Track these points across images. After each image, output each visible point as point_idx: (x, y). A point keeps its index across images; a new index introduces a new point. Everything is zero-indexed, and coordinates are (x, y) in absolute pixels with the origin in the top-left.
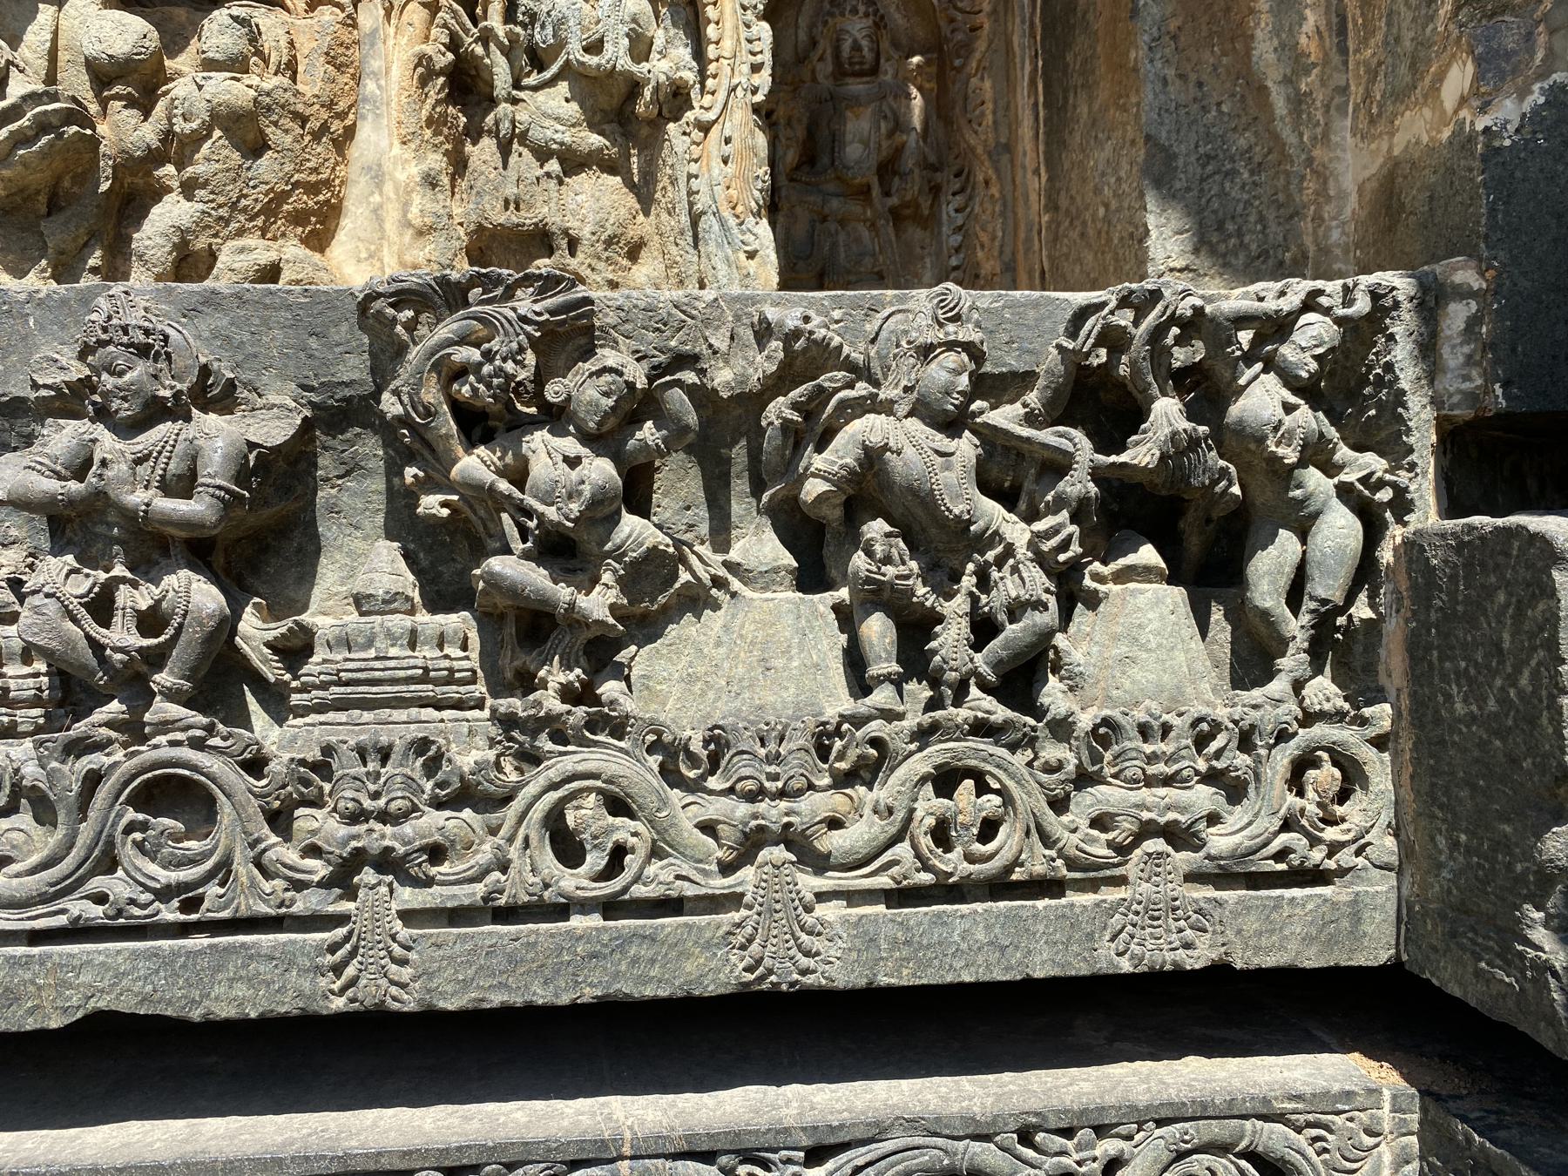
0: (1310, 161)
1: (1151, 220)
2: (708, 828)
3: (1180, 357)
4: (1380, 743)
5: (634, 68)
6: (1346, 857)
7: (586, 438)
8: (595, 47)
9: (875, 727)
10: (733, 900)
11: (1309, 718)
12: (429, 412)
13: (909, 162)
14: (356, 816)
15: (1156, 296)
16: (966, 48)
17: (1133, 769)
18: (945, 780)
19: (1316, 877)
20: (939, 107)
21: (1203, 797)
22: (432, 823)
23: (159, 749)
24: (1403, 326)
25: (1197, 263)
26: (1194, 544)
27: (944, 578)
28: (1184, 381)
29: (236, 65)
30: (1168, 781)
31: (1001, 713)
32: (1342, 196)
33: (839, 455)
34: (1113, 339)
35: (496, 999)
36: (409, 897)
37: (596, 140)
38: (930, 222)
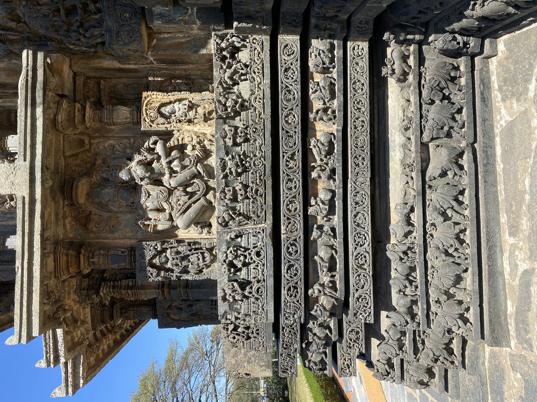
8: (185, 109)
13: (187, 82)
16: (173, 74)
18: (255, 73)
19: (263, 42)
20: (178, 79)
21: (256, 51)
22: (257, 112)
23: (251, 132)
24: (217, 33)
26: (235, 51)
27: (238, 72)
28: (221, 52)
29: (192, 137)
34: (219, 57)
36: (262, 114)
38: (194, 79)
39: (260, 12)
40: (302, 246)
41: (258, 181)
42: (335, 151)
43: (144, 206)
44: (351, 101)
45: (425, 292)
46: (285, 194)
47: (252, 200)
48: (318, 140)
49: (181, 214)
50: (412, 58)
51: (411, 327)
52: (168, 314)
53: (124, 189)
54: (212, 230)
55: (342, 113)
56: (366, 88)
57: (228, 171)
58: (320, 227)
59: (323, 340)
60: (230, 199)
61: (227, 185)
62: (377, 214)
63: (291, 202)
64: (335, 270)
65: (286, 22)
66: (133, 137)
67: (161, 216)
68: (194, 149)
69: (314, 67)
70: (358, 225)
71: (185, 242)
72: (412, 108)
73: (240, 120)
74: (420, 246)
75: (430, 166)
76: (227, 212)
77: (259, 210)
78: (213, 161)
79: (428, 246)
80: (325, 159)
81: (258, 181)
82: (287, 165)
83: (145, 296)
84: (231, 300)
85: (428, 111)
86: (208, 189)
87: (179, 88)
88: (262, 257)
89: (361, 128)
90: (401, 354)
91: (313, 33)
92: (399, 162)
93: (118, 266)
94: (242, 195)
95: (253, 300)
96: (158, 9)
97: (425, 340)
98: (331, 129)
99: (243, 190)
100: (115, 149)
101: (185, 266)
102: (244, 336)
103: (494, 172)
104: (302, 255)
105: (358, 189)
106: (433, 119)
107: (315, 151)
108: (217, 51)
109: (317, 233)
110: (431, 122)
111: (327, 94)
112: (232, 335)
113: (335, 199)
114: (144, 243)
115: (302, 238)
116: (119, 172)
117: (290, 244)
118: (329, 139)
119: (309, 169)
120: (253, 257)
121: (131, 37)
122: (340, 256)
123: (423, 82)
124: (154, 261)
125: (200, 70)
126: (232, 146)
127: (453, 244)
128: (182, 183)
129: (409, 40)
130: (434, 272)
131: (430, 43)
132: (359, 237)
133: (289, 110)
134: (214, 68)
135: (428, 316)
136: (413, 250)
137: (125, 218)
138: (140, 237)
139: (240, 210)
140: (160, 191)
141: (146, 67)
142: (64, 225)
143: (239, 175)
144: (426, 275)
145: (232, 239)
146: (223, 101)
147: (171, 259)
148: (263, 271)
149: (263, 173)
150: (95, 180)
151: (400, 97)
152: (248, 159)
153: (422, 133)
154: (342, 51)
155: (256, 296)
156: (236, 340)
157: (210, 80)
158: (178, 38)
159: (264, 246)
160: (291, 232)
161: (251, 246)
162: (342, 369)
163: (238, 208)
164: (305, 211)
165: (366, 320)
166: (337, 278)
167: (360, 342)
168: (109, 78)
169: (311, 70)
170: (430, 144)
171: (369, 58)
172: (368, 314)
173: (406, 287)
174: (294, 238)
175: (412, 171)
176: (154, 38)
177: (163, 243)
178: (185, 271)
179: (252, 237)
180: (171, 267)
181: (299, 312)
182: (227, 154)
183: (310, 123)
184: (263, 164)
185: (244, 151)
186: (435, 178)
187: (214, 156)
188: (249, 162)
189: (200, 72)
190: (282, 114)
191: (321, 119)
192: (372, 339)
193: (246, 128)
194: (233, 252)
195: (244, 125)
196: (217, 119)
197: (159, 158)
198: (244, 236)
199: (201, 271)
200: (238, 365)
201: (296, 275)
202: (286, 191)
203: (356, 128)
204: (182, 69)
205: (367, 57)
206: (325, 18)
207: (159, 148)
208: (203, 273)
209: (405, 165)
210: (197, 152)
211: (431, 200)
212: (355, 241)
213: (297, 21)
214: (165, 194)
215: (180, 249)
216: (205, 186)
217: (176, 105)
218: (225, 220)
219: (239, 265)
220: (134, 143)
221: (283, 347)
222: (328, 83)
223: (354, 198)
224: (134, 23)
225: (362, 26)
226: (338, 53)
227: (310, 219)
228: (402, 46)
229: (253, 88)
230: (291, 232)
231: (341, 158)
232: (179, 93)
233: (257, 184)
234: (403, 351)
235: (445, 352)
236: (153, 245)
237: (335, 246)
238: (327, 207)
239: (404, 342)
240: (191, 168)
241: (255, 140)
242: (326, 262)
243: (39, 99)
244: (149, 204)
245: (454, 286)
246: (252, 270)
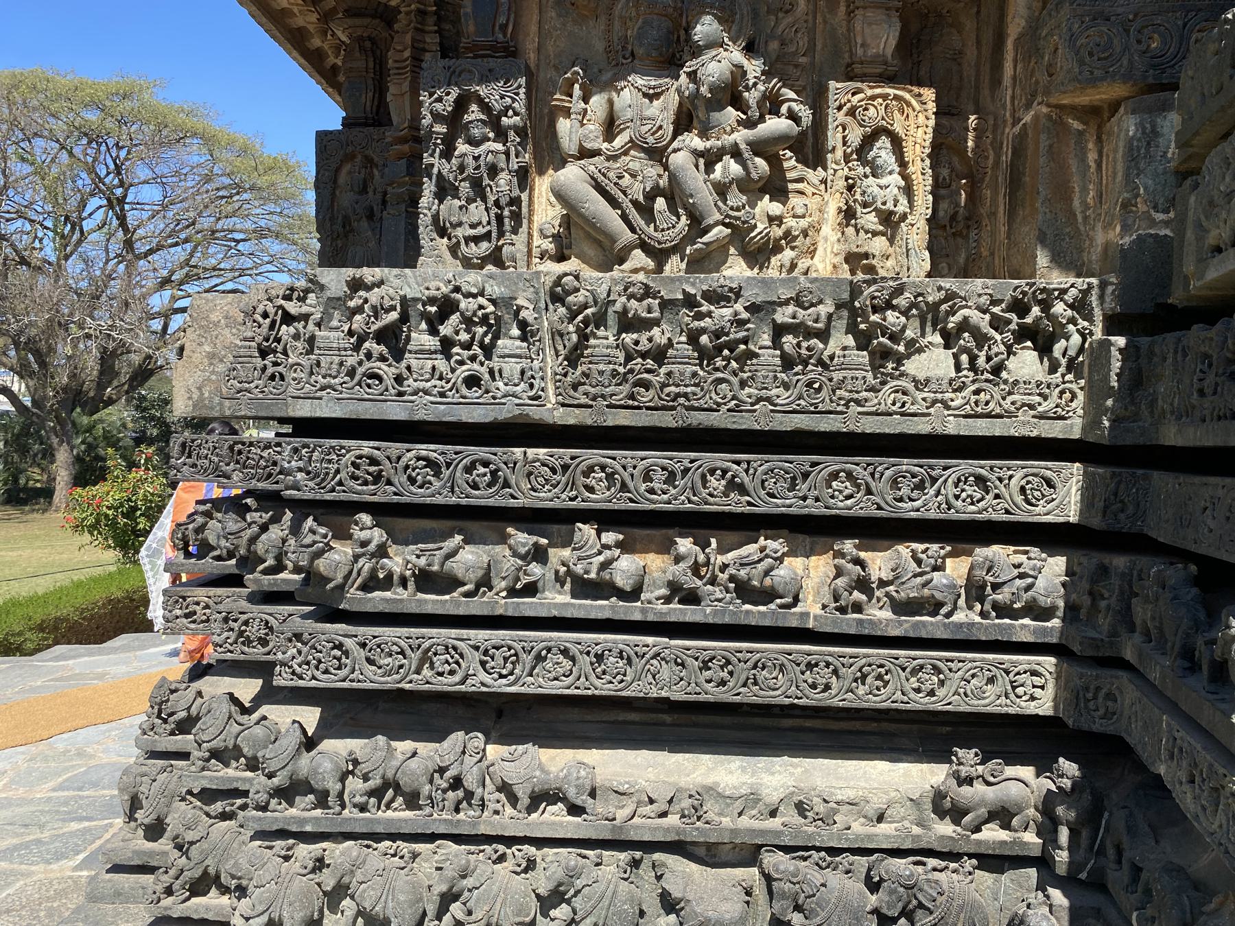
0: (1088, 236)
1: (1038, 253)
2: (924, 399)
3: (1040, 297)
4: (1081, 389)
5: (895, 209)
6: (1071, 414)
7: (900, 313)
8: (884, 203)
9: (963, 379)
10: (929, 415)
11: (1064, 383)
12: (867, 306)
13: (960, 218)
14: (851, 391)
15: (1035, 283)
16: (982, 180)
17: (1021, 391)
18: (977, 392)
20: (970, 197)
21: (1038, 399)
22: (864, 394)
24: (1095, 292)
25: (1051, 265)
26: (1040, 342)
27: (980, 348)
28: (1039, 302)
29: (803, 216)
30: (1029, 394)
31: (992, 377)
32: (1097, 246)
33: (958, 318)
34: (1024, 293)
35: (878, 431)
36: (860, 409)
37: (881, 228)
38: (966, 237)
39: (1152, 412)
40: (491, 502)
41: (672, 389)
42: (747, 607)
43: (623, 84)
44: (884, 657)
45: (348, 830)
46: (634, 462)
47: (621, 370)
48: (780, 560)
49: (592, 178)
50: (1004, 835)
51: (257, 783)
52: (350, 157)
53: (670, 32)
54: (549, 261)
55: (852, 631)
56: (921, 702)
57: (704, 309)
58: (539, 555)
59: (249, 550)
60: (625, 310)
61: (665, 305)
62: (574, 714)
63: (610, 477)
64: (420, 589)
65: (1119, 482)
66: (812, 64)
67: (594, 128)
68: (773, 220)
69: (986, 559)
70: (539, 659)
71: (522, 190)
72: (858, 827)
73: (845, 348)
74: (474, 825)
75: (694, 866)
76: (591, 300)
77: (592, 390)
78: (736, 270)
79: (472, 848)
80: (725, 576)
81: (672, 389)
82: (712, 472)
83: (395, 90)
84: (352, 304)
85: (847, 872)
86: (660, 255)
87: (943, 198)
88: (464, 391)
89: (810, 681)
90: (201, 754)
91: (1084, 560)
92: (709, 781)
93: (466, 14)
94: (637, 343)
95: (351, 361)
96: (1171, 123)
97: (234, 822)
98: (811, 598)
99: (649, 346)
100: (781, 15)
101: (457, 189)
102: (267, 340)
104: (464, 501)
105: (639, 664)
106: (823, 885)
107: (750, 549)
108: (1044, 290)
109: (524, 545)
110: (816, 877)
111: (911, 590)
112: (271, 310)
113: (614, 599)
114: (523, 81)
115: (512, 503)
116: (713, 15)
117: (497, 470)
118: (780, 590)
119: (702, 532)
120: (465, 367)
121: (1091, 54)
122: (458, 604)
123: (932, 862)
124: (474, 107)
125: (992, 254)
126: (773, 320)
127: (473, 917)
128: (679, 184)
129: (1056, 831)
130: (402, 857)
131: (1044, 890)
132: (506, 659)
133: (867, 484)
134: (993, 281)
135: (282, 834)
136: (464, 804)
137: (595, 38)
138: (542, 75)
139: (596, 337)
140: (660, 127)
141: (1005, 109)
143: (693, 338)
144: (393, 837)
145: (517, 313)
146: (901, 301)
147: (477, 151)
148: (426, 392)
151: (893, 794)
152: (734, 364)
153: (787, 849)
154: (1029, 638)
155: (360, 370)
156: (260, 319)
157: (965, 273)
158: (1085, 190)
159: (494, 398)
160: (529, 474)
161: (495, 363)
162: (184, 598)
163: (601, 333)
164: (587, 516)
165: (283, 664)
166: (399, 594)
167: (239, 647)
168: (978, 12)
169: (978, 550)
170: (755, 870)
171: (1007, 715)
172: (298, 670)
173: (366, 778)
174: (513, 482)
175: (683, 816)
176: (1084, 124)
177: (521, 132)
178: (445, 190)
179: (519, 367)
180: (456, 153)
181: (311, 484)
182: (753, 308)
183: (829, 540)
184: (719, 404)
185: (757, 356)
186: (659, 878)
187: (749, 273)
188: (725, 367)
189: (985, 253)
190: (859, 466)
191: (839, 573)
192: (260, 682)
193: (821, 362)
194: (480, 313)
195: (832, 358)
196: (852, 282)
197: (750, 124)
198: (525, 344)
199: (442, 232)
200: (206, 329)
201: (412, 480)
202: (642, 465)
203: (810, 666)
204: (997, 206)
205: (1011, 711)
206: (1127, 597)
207: (776, 125)
208: (435, 235)
209: (699, 799)
210: (760, 227)
211: (598, 864)
212: (497, 648)
213: (1122, 516)
214: (651, 140)
215: (503, 179)
216: (669, 245)
217: (895, 180)
218: (568, 293)
219: (445, 330)
220: (796, 66)
221: (236, 443)
222: (939, 596)
223: (615, 652)
224: (1131, 62)
225: (1100, 700)
226: (1025, 629)
227: (564, 528)
228: (1037, 809)
229: (934, 387)
230: (529, 474)
231: (727, 620)
232: (929, 188)
233: (664, 385)
234: (208, 760)
235: (197, 873)
236: (516, 105)
237: (485, 593)
238: (593, 575)
239: (234, 764)
240: (719, 209)
241: (786, 386)
242: (442, 565)
244: (627, 97)
245: (360, 913)
246: (429, 364)
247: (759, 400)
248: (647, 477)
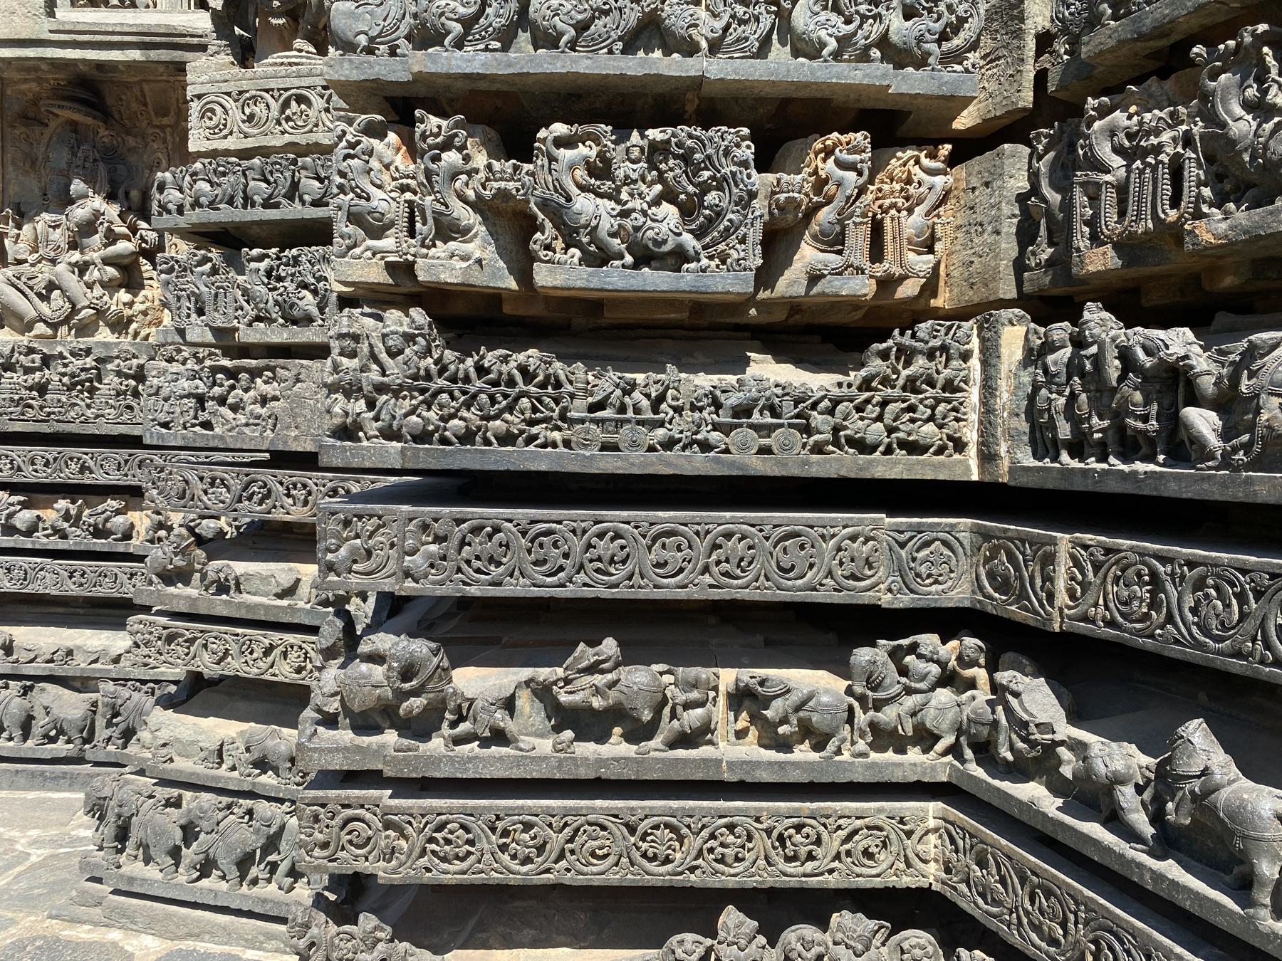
29: (144, 302)
42: (95, 540)
75: (67, 691)
78: (104, 334)
81: (47, 410)
86: (54, 326)
103: (31, 788)
107: (100, 508)
137: (34, 185)
142: (26, 81)
149: (61, 418)
150: (100, 135)
163: (8, 374)
185: (99, 389)
188: (77, 396)
210: (114, 308)
231: (82, 548)
233: (41, 408)
243: (154, 55)
247: (97, 417)
248: (33, 464)
